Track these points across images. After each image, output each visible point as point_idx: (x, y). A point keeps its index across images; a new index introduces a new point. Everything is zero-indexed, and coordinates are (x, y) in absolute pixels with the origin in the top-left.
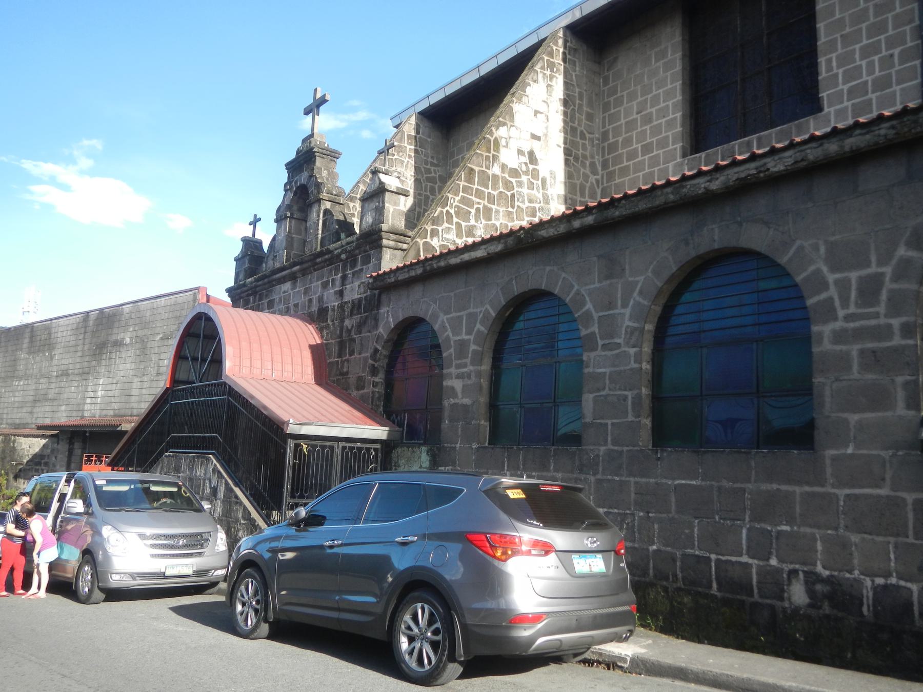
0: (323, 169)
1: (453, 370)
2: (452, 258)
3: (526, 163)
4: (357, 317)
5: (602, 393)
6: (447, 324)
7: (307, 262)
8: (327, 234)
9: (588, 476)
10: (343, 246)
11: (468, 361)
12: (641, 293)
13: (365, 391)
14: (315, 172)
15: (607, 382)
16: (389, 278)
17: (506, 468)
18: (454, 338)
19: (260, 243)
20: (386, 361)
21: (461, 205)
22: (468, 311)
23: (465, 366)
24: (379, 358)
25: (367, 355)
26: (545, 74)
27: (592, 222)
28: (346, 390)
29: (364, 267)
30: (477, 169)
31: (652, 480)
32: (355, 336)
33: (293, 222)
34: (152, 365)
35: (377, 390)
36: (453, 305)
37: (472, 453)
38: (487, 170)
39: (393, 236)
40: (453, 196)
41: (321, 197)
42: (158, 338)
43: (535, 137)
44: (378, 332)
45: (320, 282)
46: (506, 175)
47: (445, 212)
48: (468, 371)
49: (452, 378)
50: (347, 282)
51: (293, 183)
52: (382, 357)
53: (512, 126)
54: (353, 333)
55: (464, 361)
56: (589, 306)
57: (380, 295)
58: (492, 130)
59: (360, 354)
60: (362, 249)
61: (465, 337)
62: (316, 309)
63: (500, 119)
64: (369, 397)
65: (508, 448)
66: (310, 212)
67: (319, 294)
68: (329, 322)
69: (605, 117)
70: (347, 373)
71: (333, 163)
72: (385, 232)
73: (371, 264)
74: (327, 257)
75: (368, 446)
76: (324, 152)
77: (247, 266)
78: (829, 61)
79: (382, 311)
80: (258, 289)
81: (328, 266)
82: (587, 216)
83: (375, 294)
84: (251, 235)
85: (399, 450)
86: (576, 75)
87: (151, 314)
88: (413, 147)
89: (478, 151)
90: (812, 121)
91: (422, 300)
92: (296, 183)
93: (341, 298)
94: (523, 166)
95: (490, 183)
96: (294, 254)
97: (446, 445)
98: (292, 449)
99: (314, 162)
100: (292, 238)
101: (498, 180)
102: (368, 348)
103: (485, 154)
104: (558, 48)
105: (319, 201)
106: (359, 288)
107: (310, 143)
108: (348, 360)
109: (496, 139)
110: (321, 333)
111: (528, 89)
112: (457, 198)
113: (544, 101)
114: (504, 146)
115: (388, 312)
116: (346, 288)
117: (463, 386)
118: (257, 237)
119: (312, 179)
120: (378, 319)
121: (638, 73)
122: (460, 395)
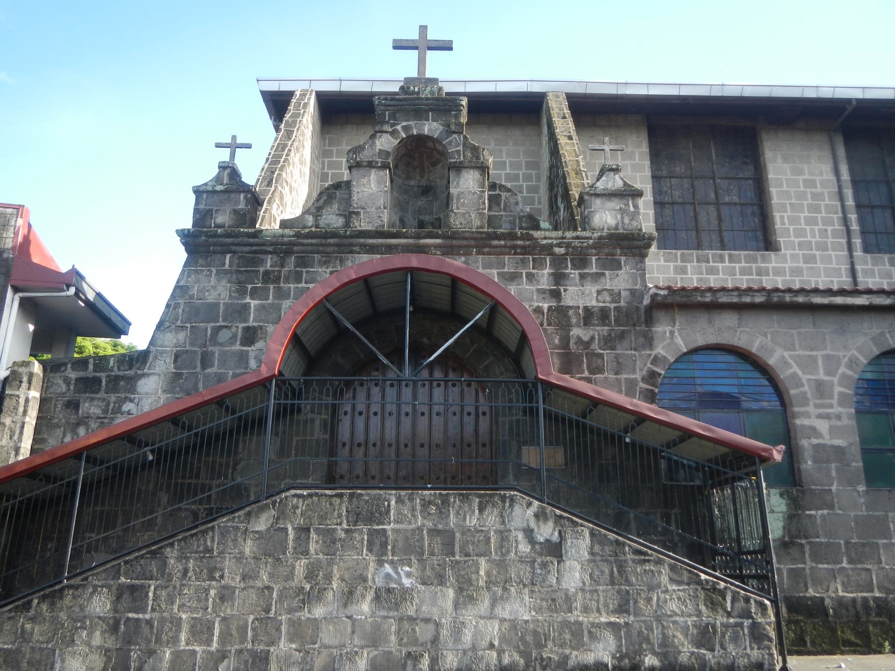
1: (811, 409)
6: (790, 361)
10: (565, 238)
11: (835, 401)
16: (701, 296)
18: (805, 378)
23: (831, 406)
29: (607, 272)
37: (859, 495)
44: (654, 353)
49: (810, 417)
50: (568, 283)
55: (828, 401)
61: (822, 376)
74: (519, 242)
78: (782, 218)
80: (295, 248)
81: (515, 254)
90: (773, 255)
91: (739, 330)
97: (814, 487)
115: (672, 333)
116: (565, 290)
117: (831, 427)
120: (652, 339)
122: (826, 435)
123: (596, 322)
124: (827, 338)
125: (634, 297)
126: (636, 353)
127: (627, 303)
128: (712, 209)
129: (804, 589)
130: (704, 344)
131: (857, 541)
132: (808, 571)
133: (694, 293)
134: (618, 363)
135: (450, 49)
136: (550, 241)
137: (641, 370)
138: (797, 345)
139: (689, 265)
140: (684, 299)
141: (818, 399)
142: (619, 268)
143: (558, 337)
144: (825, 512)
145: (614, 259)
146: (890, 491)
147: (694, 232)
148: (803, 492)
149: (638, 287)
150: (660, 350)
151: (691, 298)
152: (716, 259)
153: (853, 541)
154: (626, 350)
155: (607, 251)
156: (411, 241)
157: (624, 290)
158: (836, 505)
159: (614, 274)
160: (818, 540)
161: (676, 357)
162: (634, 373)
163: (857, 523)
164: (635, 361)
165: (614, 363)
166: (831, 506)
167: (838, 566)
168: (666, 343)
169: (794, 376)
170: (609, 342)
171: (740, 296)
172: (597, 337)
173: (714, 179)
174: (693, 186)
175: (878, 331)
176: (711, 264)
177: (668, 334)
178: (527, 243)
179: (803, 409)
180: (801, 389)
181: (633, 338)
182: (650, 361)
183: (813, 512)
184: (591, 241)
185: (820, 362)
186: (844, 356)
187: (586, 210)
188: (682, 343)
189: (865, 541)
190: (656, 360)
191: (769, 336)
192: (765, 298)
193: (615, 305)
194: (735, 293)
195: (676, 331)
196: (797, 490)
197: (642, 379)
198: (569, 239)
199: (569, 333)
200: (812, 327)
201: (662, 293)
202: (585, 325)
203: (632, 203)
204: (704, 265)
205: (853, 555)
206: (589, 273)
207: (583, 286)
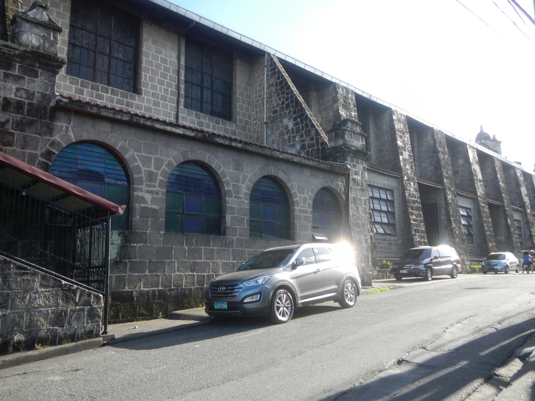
1: (143, 187)
5: (234, 215)
6: (137, 158)
9: (229, 248)
11: (157, 184)
12: (249, 180)
15: (236, 211)
16: (90, 109)
17: (185, 245)
18: (143, 169)
23: (155, 187)
27: (240, 147)
29: (26, 77)
31: (253, 250)
36: (142, 148)
37: (161, 236)
44: (52, 139)
48: (157, 190)
49: (142, 192)
55: (153, 184)
56: (228, 178)
61: (152, 169)
65: (186, 235)
78: (146, 76)
82: (239, 143)
90: (137, 96)
91: (110, 135)
97: (138, 231)
115: (67, 128)
117: (152, 198)
120: (53, 129)
122: (149, 203)
123: (12, 110)
124: (159, 148)
125: (44, 99)
126: (40, 136)
127: (38, 102)
128: (106, 58)
129: (123, 287)
130: (87, 139)
131: (155, 260)
132: (127, 277)
133: (86, 106)
134: (25, 141)
137: (41, 149)
138: (142, 150)
139: (85, 90)
140: (79, 108)
141: (148, 182)
142: (36, 76)
144: (142, 244)
145: (34, 70)
146: (176, 234)
147: (92, 70)
148: (131, 233)
149: (48, 93)
150: (57, 138)
151: (83, 108)
152: (104, 90)
153: (153, 260)
154: (33, 133)
155: (28, 62)
157: (37, 92)
158: (148, 241)
159: (31, 79)
160: (135, 260)
161: (68, 144)
162: (36, 150)
163: (156, 251)
164: (38, 142)
165: (22, 141)
166: (145, 242)
167: (143, 274)
168: (62, 134)
169: (138, 167)
170: (20, 126)
171: (114, 114)
172: (11, 121)
173: (110, 41)
174: (96, 40)
175: (185, 150)
176: (100, 92)
177: (64, 128)
179: (139, 187)
180: (140, 175)
181: (39, 127)
182: (49, 144)
183: (135, 245)
185: (153, 161)
186: (166, 160)
187: (17, 29)
188: (73, 136)
189: (159, 261)
190: (53, 144)
191: (127, 141)
192: (129, 118)
193: (29, 101)
194: (112, 112)
195: (70, 128)
196: (128, 232)
197: (41, 155)
200: (152, 141)
201: (65, 100)
203: (53, 34)
204: (95, 92)
205: (152, 268)
206: (12, 74)
207: (5, 82)
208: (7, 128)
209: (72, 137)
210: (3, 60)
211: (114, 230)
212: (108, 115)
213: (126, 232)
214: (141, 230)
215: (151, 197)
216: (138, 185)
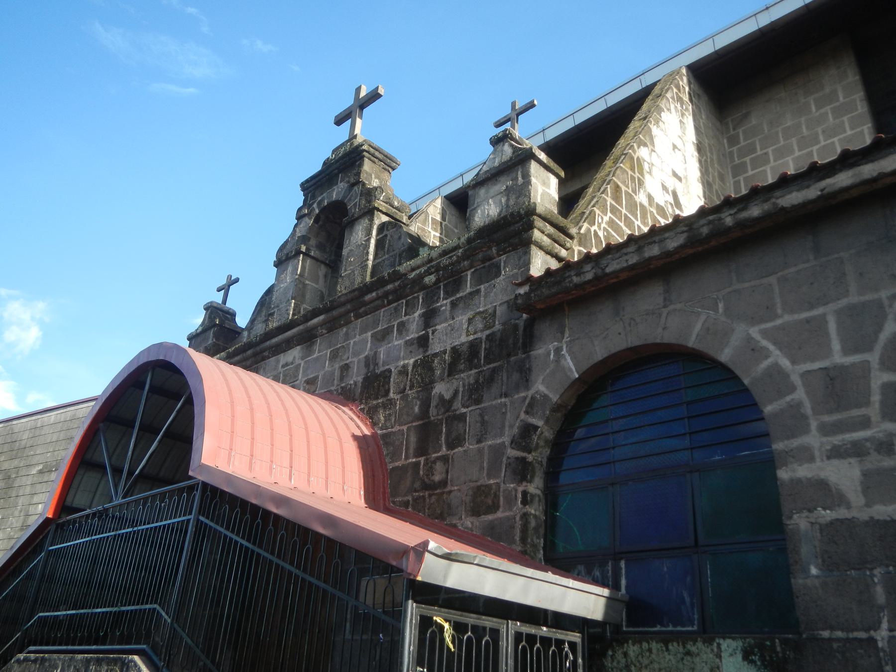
0: (373, 176)
1: (813, 439)
2: (791, 192)
3: (671, 204)
4: (468, 376)
6: (765, 343)
7: (343, 304)
8: (387, 256)
11: (874, 410)
13: (500, 514)
14: (363, 177)
16: (577, 275)
18: (794, 371)
19: (233, 315)
20: (547, 452)
21: (610, 230)
22: (844, 302)
23: (865, 423)
24: (537, 444)
25: (499, 441)
26: (676, 107)
28: (441, 517)
29: (482, 286)
30: (623, 188)
32: (464, 410)
33: (309, 261)
34: (16, 513)
35: (533, 512)
36: (778, 300)
38: (633, 194)
39: (550, 229)
40: (601, 214)
41: (376, 205)
42: (34, 471)
43: (675, 175)
45: (369, 334)
46: (655, 212)
47: (593, 233)
48: (881, 435)
49: (812, 459)
50: (437, 320)
51: (315, 205)
52: (542, 443)
53: (653, 151)
54: (457, 404)
55: (855, 412)
57: (530, 325)
58: (633, 146)
59: (479, 441)
60: (480, 256)
61: (839, 358)
62: (360, 379)
63: (641, 136)
64: (512, 527)
66: (351, 234)
67: (367, 353)
68: (391, 395)
69: (739, 181)
70: (444, 483)
71: (386, 173)
72: (540, 216)
73: (502, 277)
74: (390, 287)
75: (560, 635)
76: (377, 154)
77: (210, 342)
79: (539, 351)
81: (389, 303)
83: (516, 327)
84: (220, 301)
85: (633, 650)
86: (703, 123)
87: (31, 435)
88: (438, 235)
89: (621, 165)
91: (665, 311)
92: (319, 203)
93: (421, 350)
94: (669, 206)
95: (638, 212)
96: (304, 309)
97: (826, 634)
98: (415, 632)
99: (361, 165)
100: (305, 285)
101: (646, 214)
102: (503, 426)
103: (630, 172)
104: (684, 86)
105: (370, 212)
106: (469, 324)
107: (352, 144)
108: (445, 459)
109: (638, 158)
110: (371, 418)
111: (663, 114)
112: (606, 219)
113: (680, 137)
114: (648, 172)
115: (558, 350)
117: (865, 474)
118: (229, 304)
119: (356, 188)
120: (530, 370)
121: (788, 124)
122: (856, 498)
126: (507, 400)
135: (379, 96)
136: (417, 272)
138: (779, 305)
141: (830, 412)
143: (418, 403)
154: (495, 398)
155: (480, 256)
156: (301, 327)
159: (490, 285)
164: (504, 414)
165: (479, 424)
169: (776, 371)
171: (640, 249)
172: (461, 389)
178: (397, 284)
179: (795, 443)
180: (788, 398)
184: (461, 251)
185: (832, 326)
191: (721, 305)
196: (784, 642)
198: (436, 259)
199: (431, 393)
200: (811, 257)
202: (449, 375)
203: (522, 172)
208: (456, 408)
209: (570, 370)
210: (449, 280)
211: (724, 638)
212: (625, 265)
213: (773, 643)
214: (842, 630)
215: (856, 473)
216: (788, 438)
